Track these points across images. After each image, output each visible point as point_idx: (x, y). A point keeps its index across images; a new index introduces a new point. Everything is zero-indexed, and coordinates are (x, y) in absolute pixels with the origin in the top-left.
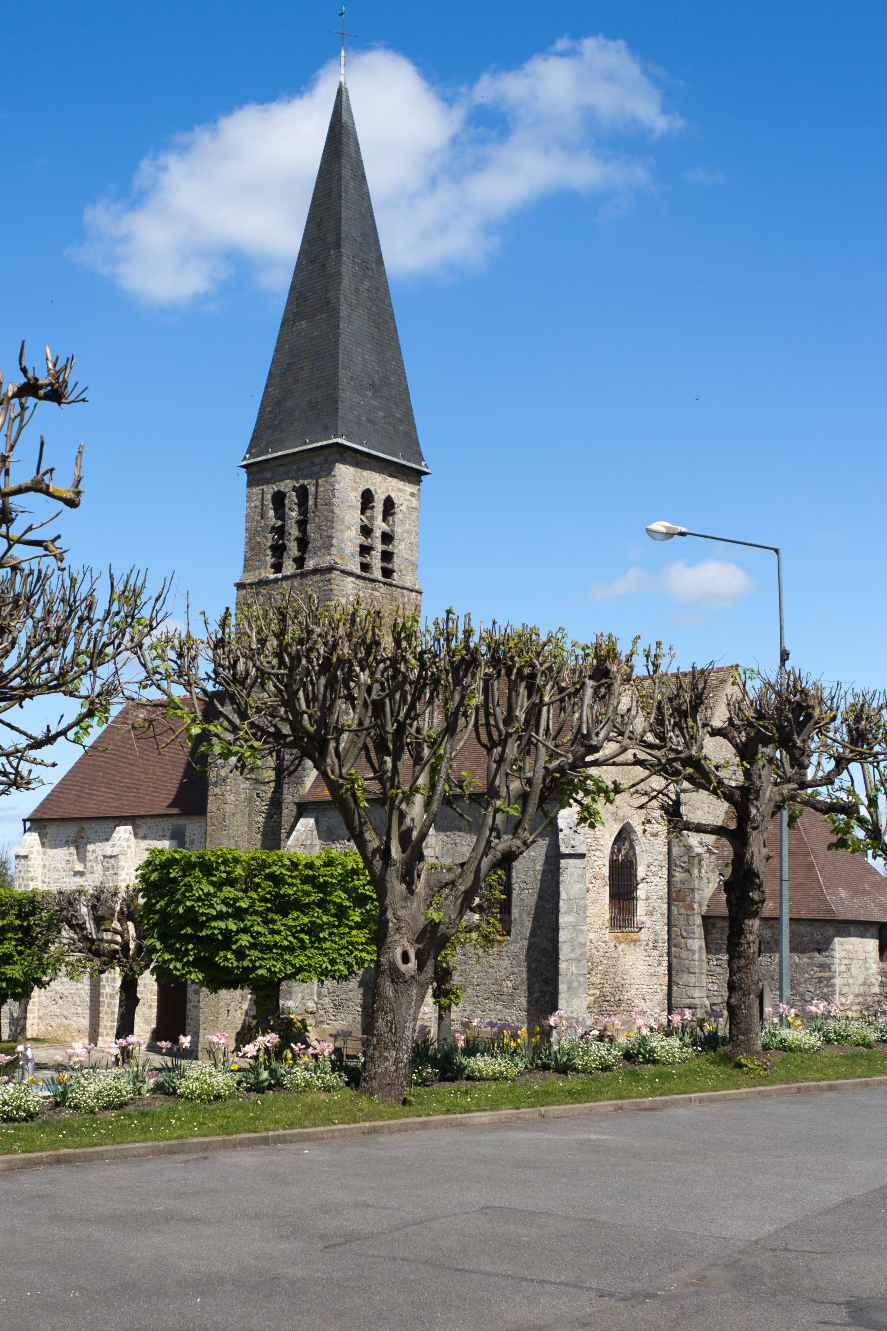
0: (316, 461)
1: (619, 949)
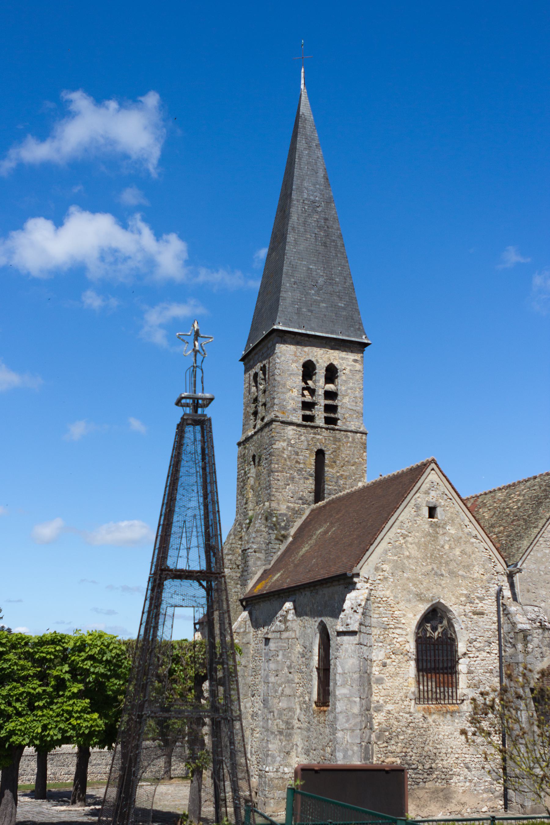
0: (269, 345)
1: (430, 720)
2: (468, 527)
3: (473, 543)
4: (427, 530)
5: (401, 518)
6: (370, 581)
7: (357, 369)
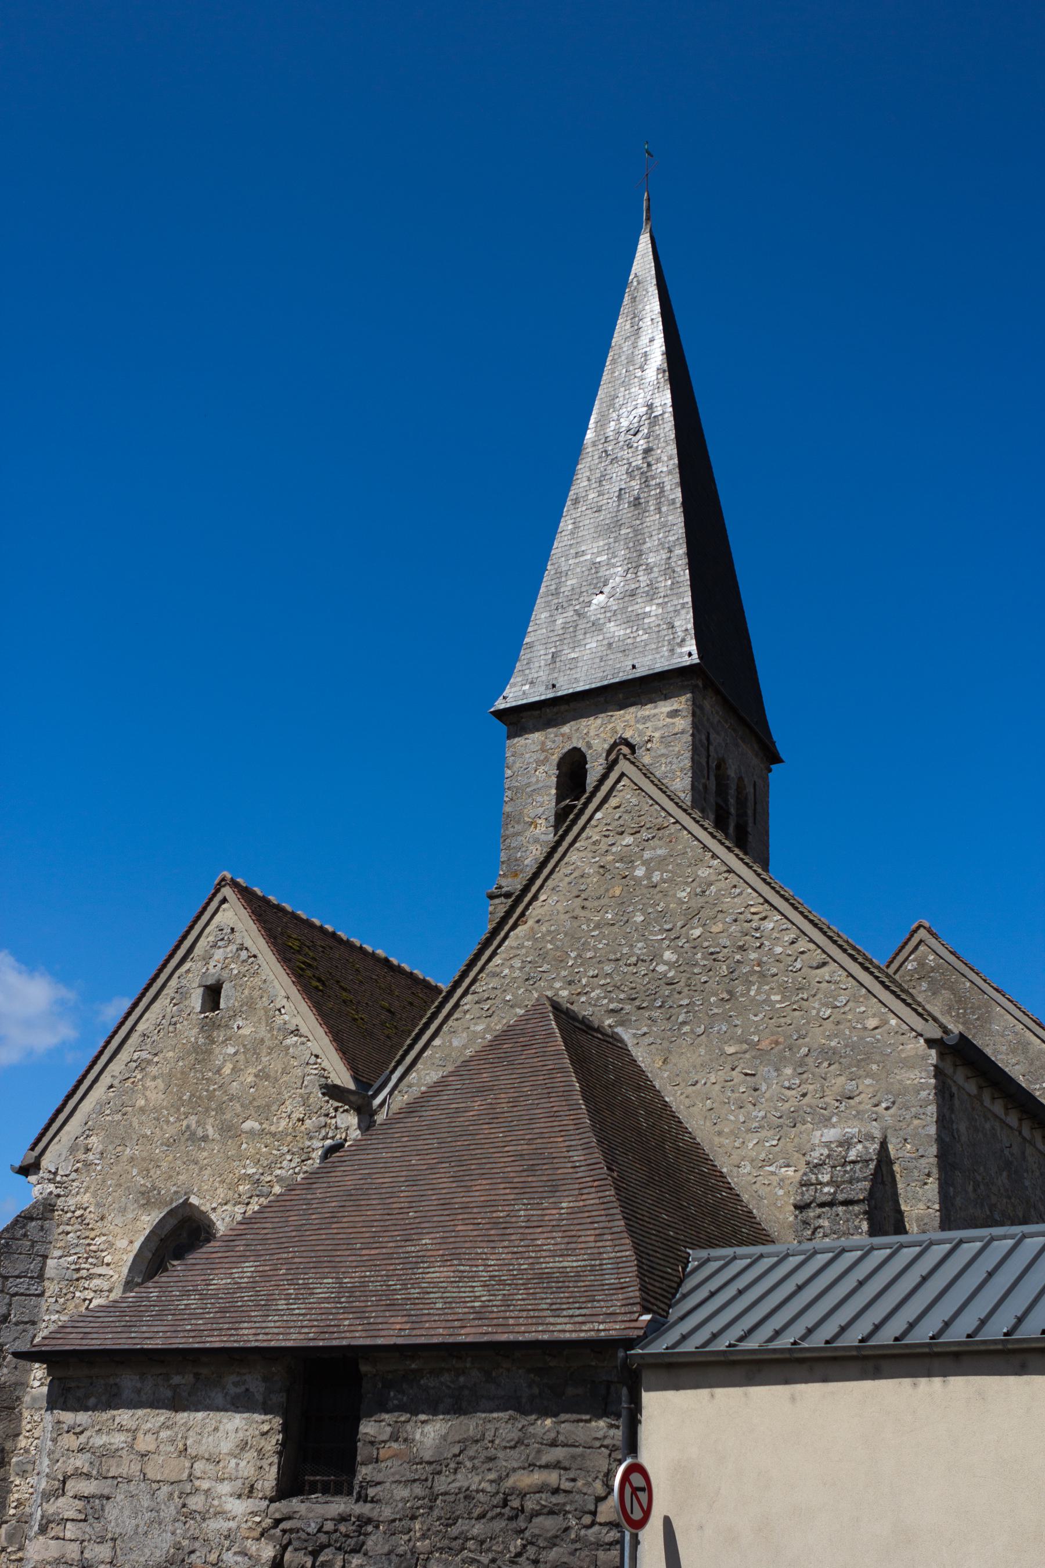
2: (283, 1011)
3: (288, 1048)
4: (193, 1039)
5: (141, 1027)
6: (58, 1178)
7: (676, 730)
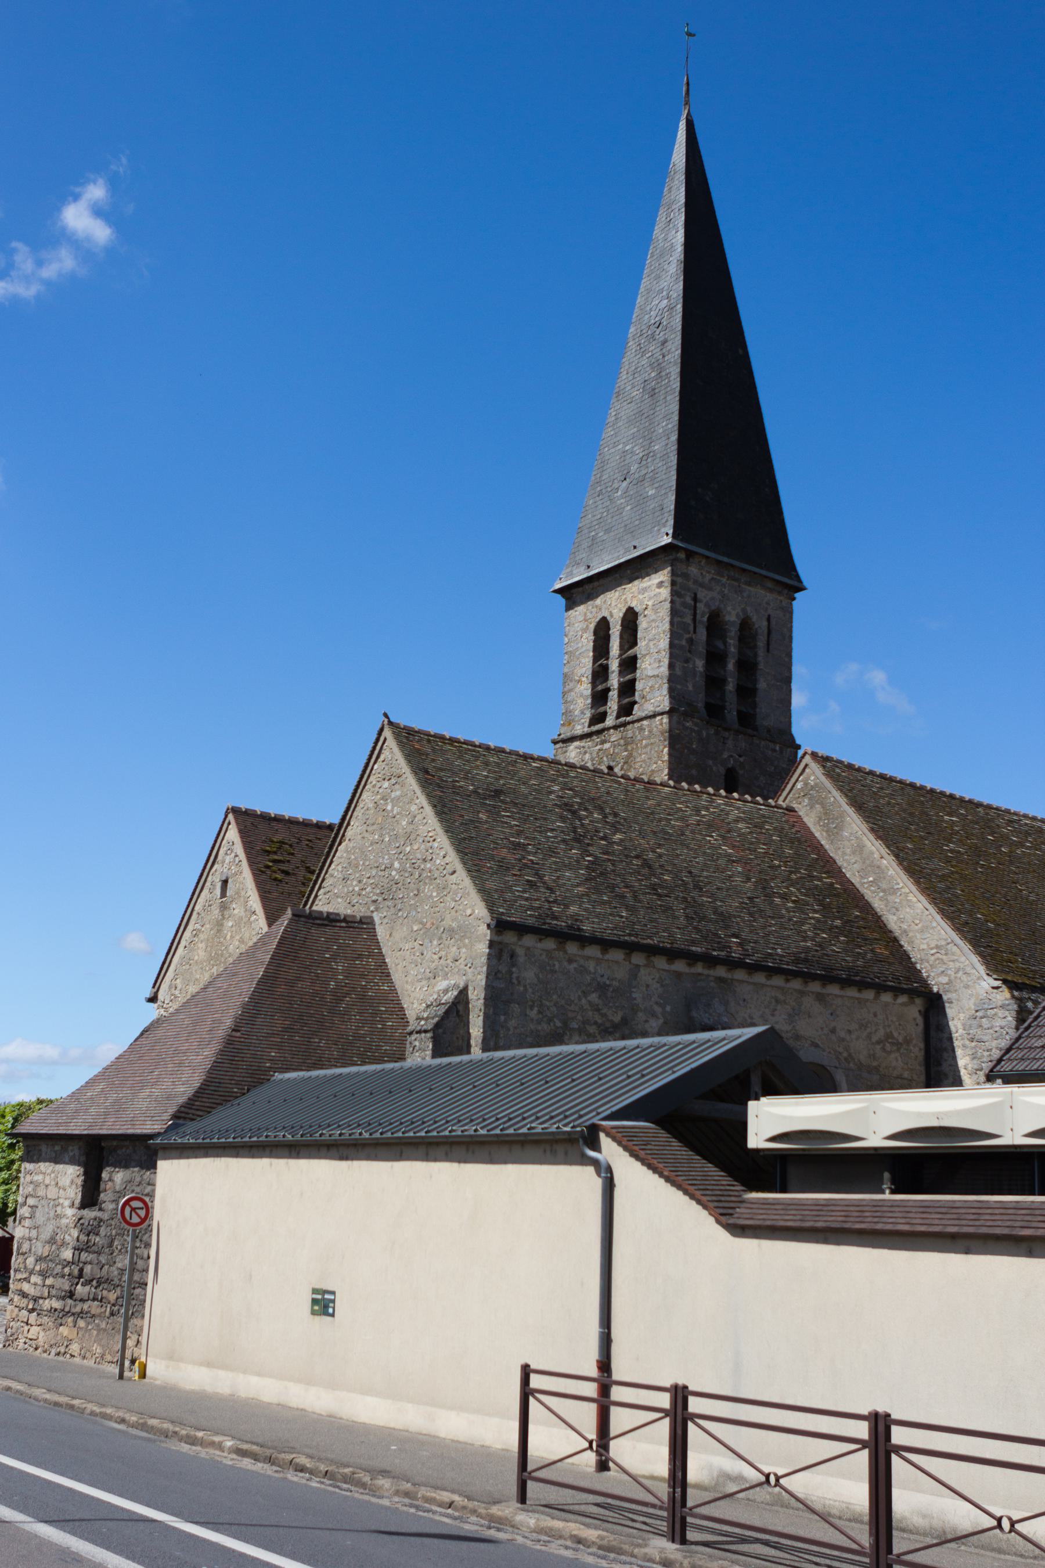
5: (197, 908)
